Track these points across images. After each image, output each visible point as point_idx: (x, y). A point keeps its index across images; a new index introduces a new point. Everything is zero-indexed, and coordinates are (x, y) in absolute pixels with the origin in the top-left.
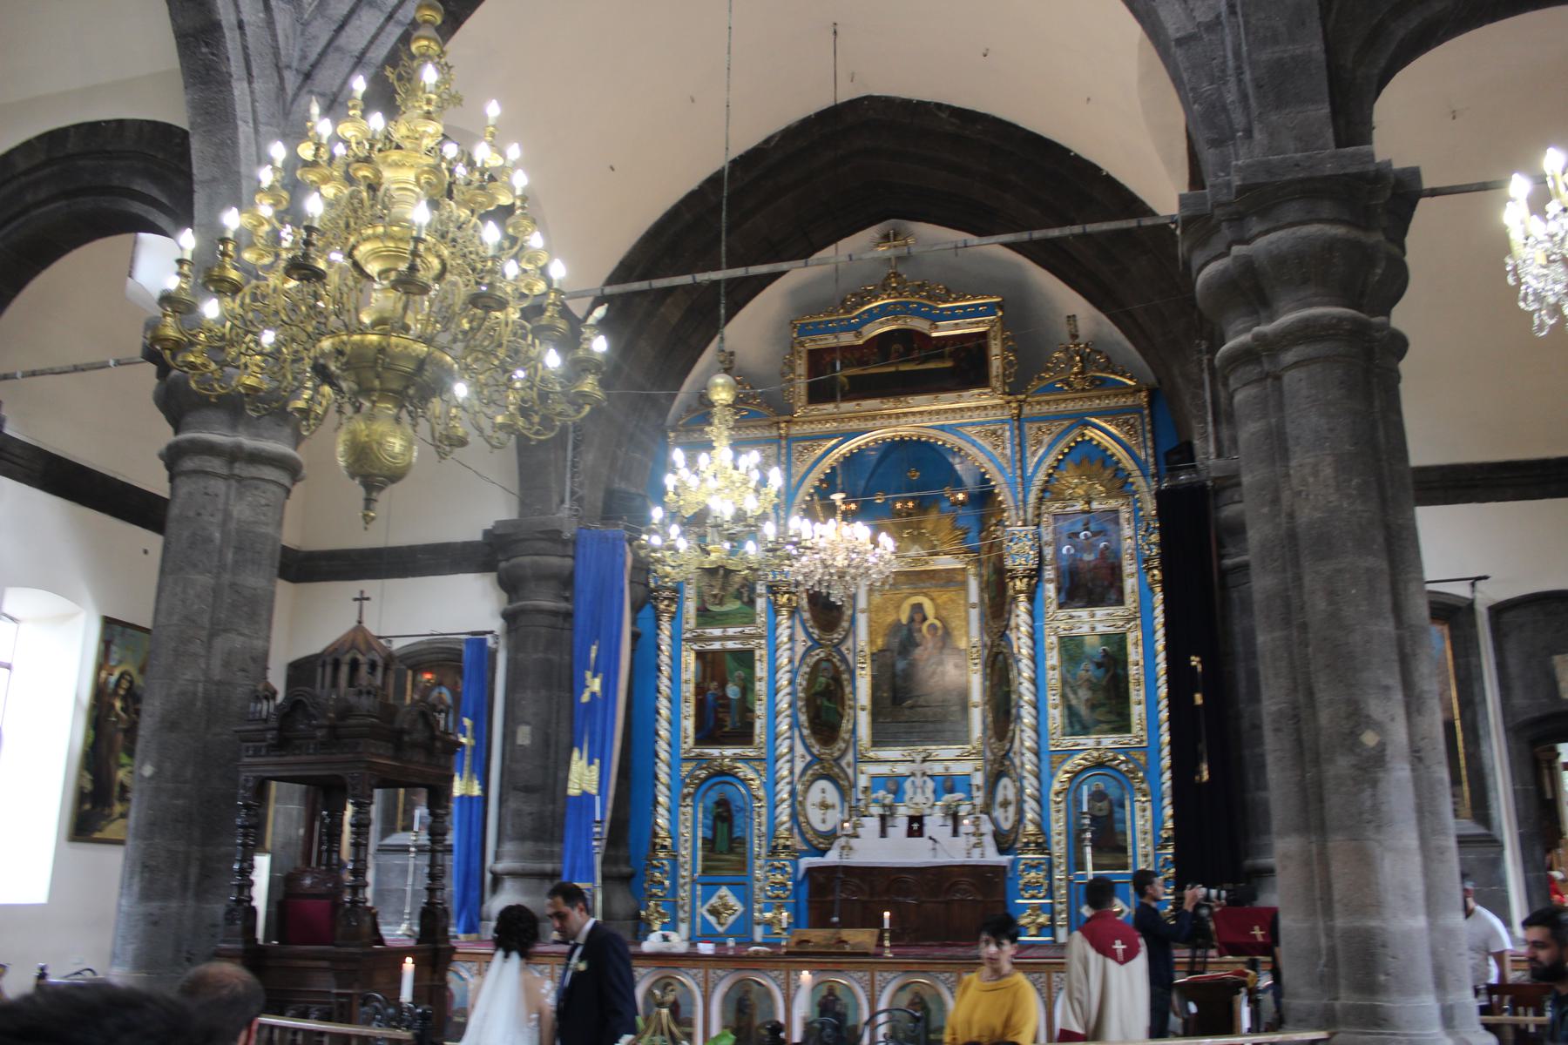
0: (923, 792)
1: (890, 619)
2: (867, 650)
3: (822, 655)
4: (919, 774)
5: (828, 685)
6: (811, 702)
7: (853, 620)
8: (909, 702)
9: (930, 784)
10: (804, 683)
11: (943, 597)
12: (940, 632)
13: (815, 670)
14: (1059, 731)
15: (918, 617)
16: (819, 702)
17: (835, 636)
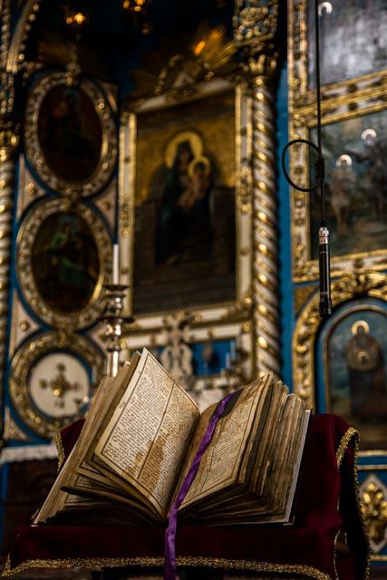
0: (180, 364)
1: (154, 164)
2: (131, 203)
3: (63, 207)
4: (176, 342)
5: (70, 244)
6: (37, 261)
7: (114, 172)
8: (172, 260)
9: (188, 354)
10: (31, 239)
11: (211, 129)
12: (207, 171)
13: (49, 224)
14: (306, 254)
15: (184, 157)
16: (55, 261)
17: (88, 186)
